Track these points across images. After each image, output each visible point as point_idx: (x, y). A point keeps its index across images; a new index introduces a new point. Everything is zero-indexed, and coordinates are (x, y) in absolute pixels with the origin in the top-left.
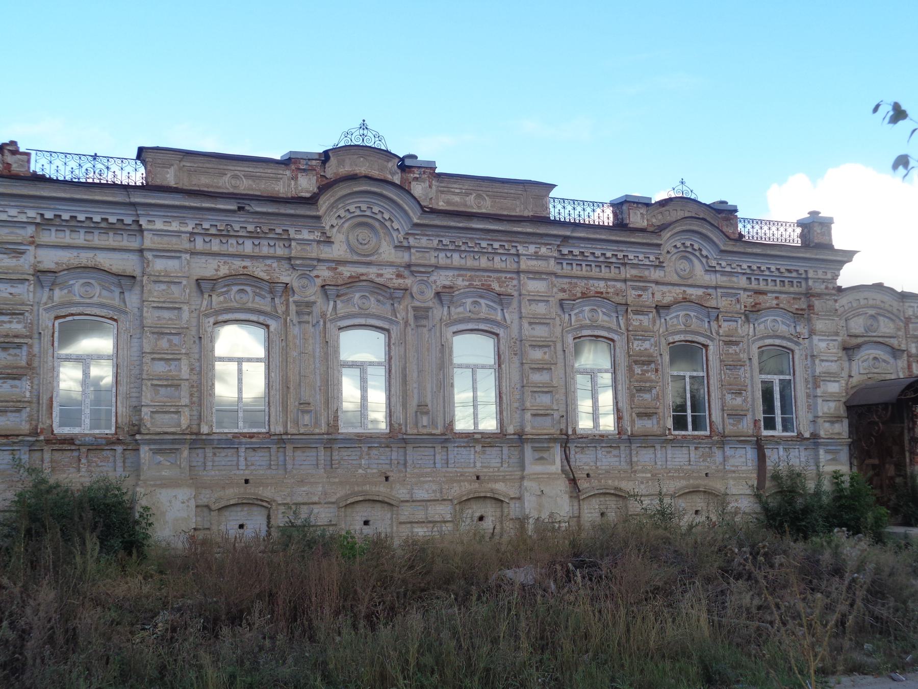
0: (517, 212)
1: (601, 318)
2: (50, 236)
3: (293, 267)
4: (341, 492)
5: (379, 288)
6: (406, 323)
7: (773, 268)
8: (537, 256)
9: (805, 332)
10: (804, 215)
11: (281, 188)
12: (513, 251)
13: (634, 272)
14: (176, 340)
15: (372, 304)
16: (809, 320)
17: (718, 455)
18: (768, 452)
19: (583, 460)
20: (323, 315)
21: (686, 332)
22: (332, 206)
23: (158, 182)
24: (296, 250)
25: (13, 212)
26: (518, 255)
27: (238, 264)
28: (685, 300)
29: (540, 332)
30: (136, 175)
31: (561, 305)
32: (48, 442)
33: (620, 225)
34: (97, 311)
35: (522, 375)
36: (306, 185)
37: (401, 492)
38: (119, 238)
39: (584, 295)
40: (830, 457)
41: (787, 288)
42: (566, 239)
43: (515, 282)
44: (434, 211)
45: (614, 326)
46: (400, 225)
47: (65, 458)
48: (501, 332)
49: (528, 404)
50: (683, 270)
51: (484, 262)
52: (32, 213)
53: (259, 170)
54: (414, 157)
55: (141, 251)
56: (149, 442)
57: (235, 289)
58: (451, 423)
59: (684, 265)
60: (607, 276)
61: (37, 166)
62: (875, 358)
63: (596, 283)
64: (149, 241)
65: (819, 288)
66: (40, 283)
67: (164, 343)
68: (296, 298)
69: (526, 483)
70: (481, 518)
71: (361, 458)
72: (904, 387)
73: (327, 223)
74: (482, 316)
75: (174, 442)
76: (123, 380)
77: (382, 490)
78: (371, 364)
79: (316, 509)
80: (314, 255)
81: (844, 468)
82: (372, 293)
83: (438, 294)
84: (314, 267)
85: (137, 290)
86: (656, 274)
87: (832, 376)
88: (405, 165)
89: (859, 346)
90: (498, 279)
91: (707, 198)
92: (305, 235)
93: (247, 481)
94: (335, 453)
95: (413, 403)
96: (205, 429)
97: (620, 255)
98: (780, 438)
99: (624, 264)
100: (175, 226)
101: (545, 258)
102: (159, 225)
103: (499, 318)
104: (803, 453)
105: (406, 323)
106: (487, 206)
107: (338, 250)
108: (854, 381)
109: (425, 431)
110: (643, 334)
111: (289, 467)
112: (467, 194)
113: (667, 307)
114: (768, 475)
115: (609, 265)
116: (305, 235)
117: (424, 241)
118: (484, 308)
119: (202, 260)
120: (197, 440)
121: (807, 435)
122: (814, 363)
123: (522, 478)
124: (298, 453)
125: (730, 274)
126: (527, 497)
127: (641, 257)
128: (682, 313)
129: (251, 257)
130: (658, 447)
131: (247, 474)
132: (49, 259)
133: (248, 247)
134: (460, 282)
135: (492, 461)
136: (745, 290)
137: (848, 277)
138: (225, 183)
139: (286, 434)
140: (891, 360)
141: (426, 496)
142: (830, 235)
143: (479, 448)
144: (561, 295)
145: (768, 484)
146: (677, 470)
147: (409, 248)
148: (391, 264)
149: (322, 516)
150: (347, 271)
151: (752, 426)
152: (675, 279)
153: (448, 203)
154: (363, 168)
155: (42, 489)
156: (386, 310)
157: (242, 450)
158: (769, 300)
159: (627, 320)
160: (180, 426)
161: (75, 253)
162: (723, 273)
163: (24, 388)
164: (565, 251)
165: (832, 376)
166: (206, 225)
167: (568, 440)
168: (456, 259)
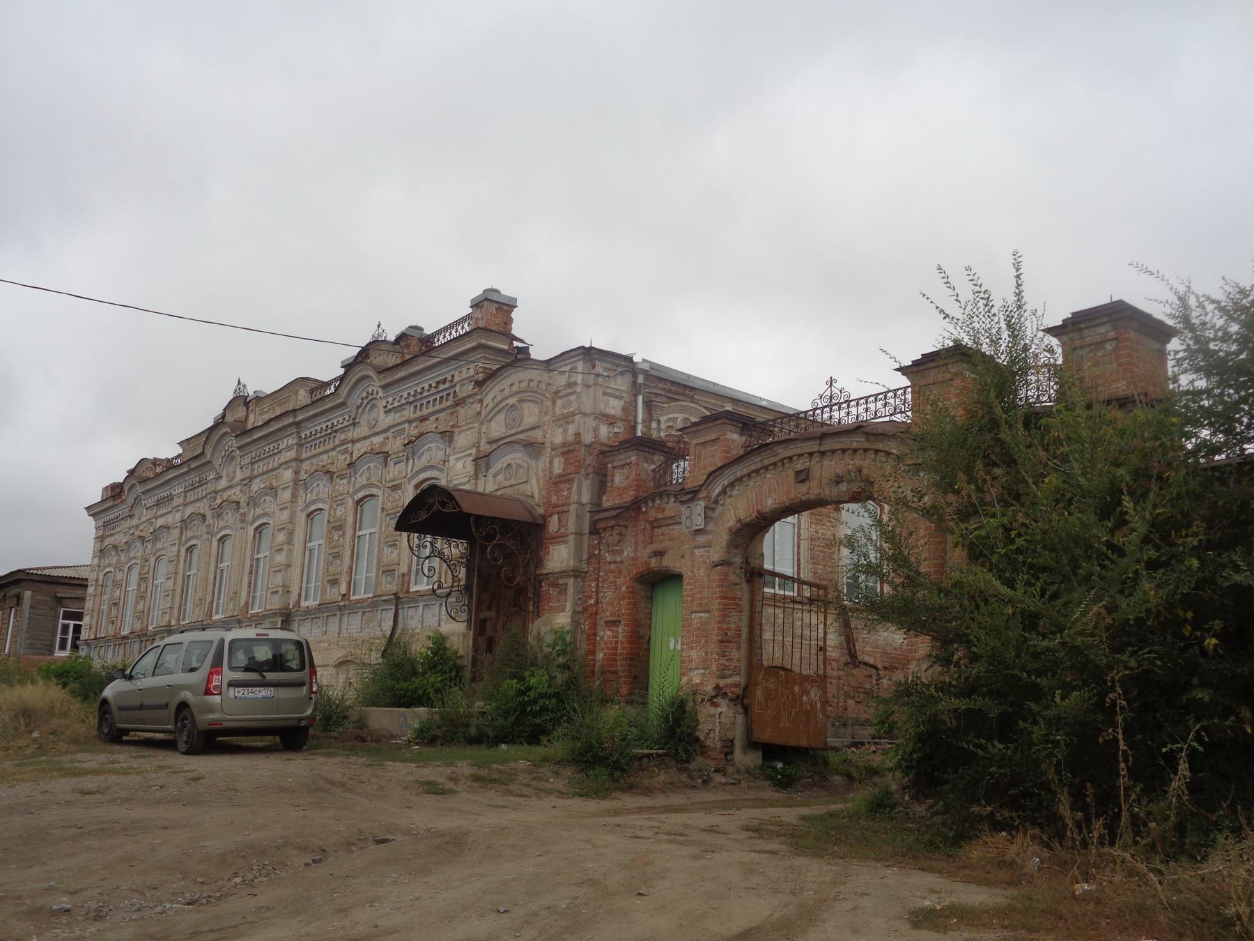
8: (289, 448)
62: (509, 465)
64: (177, 501)
73: (217, 462)
97: (329, 424)
117: (247, 460)
136: (410, 422)
158: (430, 425)
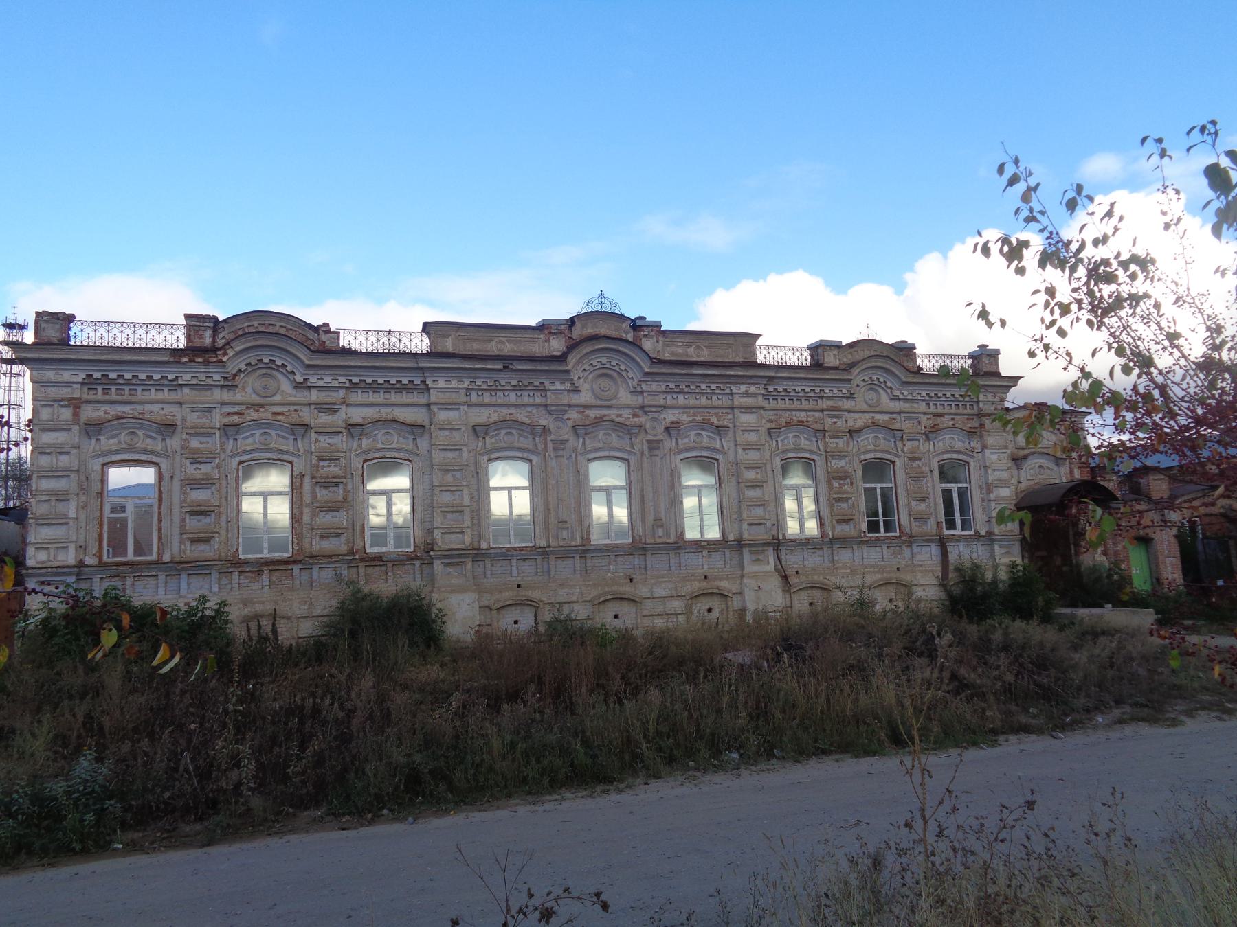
0: (730, 359)
1: (804, 442)
2: (357, 397)
3: (549, 413)
4: (594, 593)
5: (619, 426)
6: (642, 453)
7: (948, 394)
8: (747, 394)
9: (978, 447)
10: (974, 348)
11: (537, 349)
12: (728, 391)
13: (830, 403)
14: (458, 474)
15: (614, 439)
16: (981, 437)
17: (907, 552)
18: (949, 549)
19: (792, 560)
20: (575, 450)
21: (875, 451)
22: (578, 362)
23: (440, 349)
24: (551, 397)
25: (328, 379)
26: (732, 394)
27: (505, 411)
28: (874, 424)
29: (753, 456)
30: (421, 344)
31: (770, 434)
32: (362, 559)
33: (816, 365)
34: (396, 454)
35: (739, 492)
36: (557, 345)
37: (643, 591)
38: (410, 395)
39: (788, 424)
40: (1004, 551)
41: (961, 410)
42: (771, 379)
43: (730, 416)
44: (661, 362)
45: (814, 449)
46: (634, 374)
47: (376, 571)
48: (720, 457)
49: (745, 516)
50: (870, 399)
51: (704, 401)
52: (342, 380)
53: (519, 336)
54: (643, 318)
55: (428, 405)
56: (440, 557)
57: (503, 432)
58: (682, 534)
59: (871, 396)
60: (807, 407)
61: (344, 342)
62: (1040, 466)
63: (798, 414)
65: (989, 409)
66: (351, 434)
67: (449, 478)
68: (553, 437)
69: (745, 580)
70: (710, 610)
71: (609, 564)
72: (1064, 491)
73: (574, 376)
74: (704, 445)
75: (459, 556)
76: (419, 508)
77: (628, 589)
78: (615, 487)
79: (576, 607)
80: (565, 402)
81: (1019, 561)
82: (614, 430)
83: (667, 429)
84: (566, 412)
85: (426, 436)
86: (848, 404)
87: (1003, 483)
88: (637, 325)
89: (1025, 457)
90: (716, 414)
91: (889, 339)
92: (558, 386)
93: (519, 586)
94: (589, 561)
95: (650, 519)
96: (484, 545)
97: (817, 390)
98: (960, 536)
99: (821, 397)
100: (454, 384)
101: (755, 395)
102: (442, 384)
103: (718, 446)
104: (980, 548)
105: (642, 453)
106: (705, 355)
107: (585, 397)
108: (1022, 486)
109: (659, 541)
110: (839, 454)
111: (552, 573)
112: (689, 346)
113: (859, 431)
114: (951, 567)
115: (808, 398)
116: (558, 386)
117: (654, 386)
118: (705, 439)
119: (477, 409)
120: (478, 554)
121: (983, 533)
122: (986, 472)
123: (742, 576)
124: (559, 562)
125: (912, 401)
126: (747, 591)
127: (835, 390)
128: (871, 436)
129: (515, 406)
130: (855, 547)
131: (519, 580)
132: (357, 415)
133: (513, 397)
134: (685, 418)
135: (717, 562)
136: (925, 414)
137: (1015, 397)
138: (492, 348)
139: (549, 546)
140: (1055, 468)
141: (664, 594)
142: (997, 364)
143: (705, 553)
144: (769, 425)
145: (951, 575)
146: (872, 566)
147: (642, 392)
148: (628, 407)
149: (581, 612)
150: (593, 414)
151: (935, 527)
152: (865, 407)
153: (672, 354)
154: (602, 330)
155: (359, 597)
156: (625, 444)
157: (514, 561)
158: (946, 422)
159: (825, 443)
160: (464, 543)
161: (377, 409)
162: (906, 400)
163: (342, 518)
164: (771, 389)
165: (1003, 483)
166: (479, 382)
167: (779, 543)
168: (681, 400)
